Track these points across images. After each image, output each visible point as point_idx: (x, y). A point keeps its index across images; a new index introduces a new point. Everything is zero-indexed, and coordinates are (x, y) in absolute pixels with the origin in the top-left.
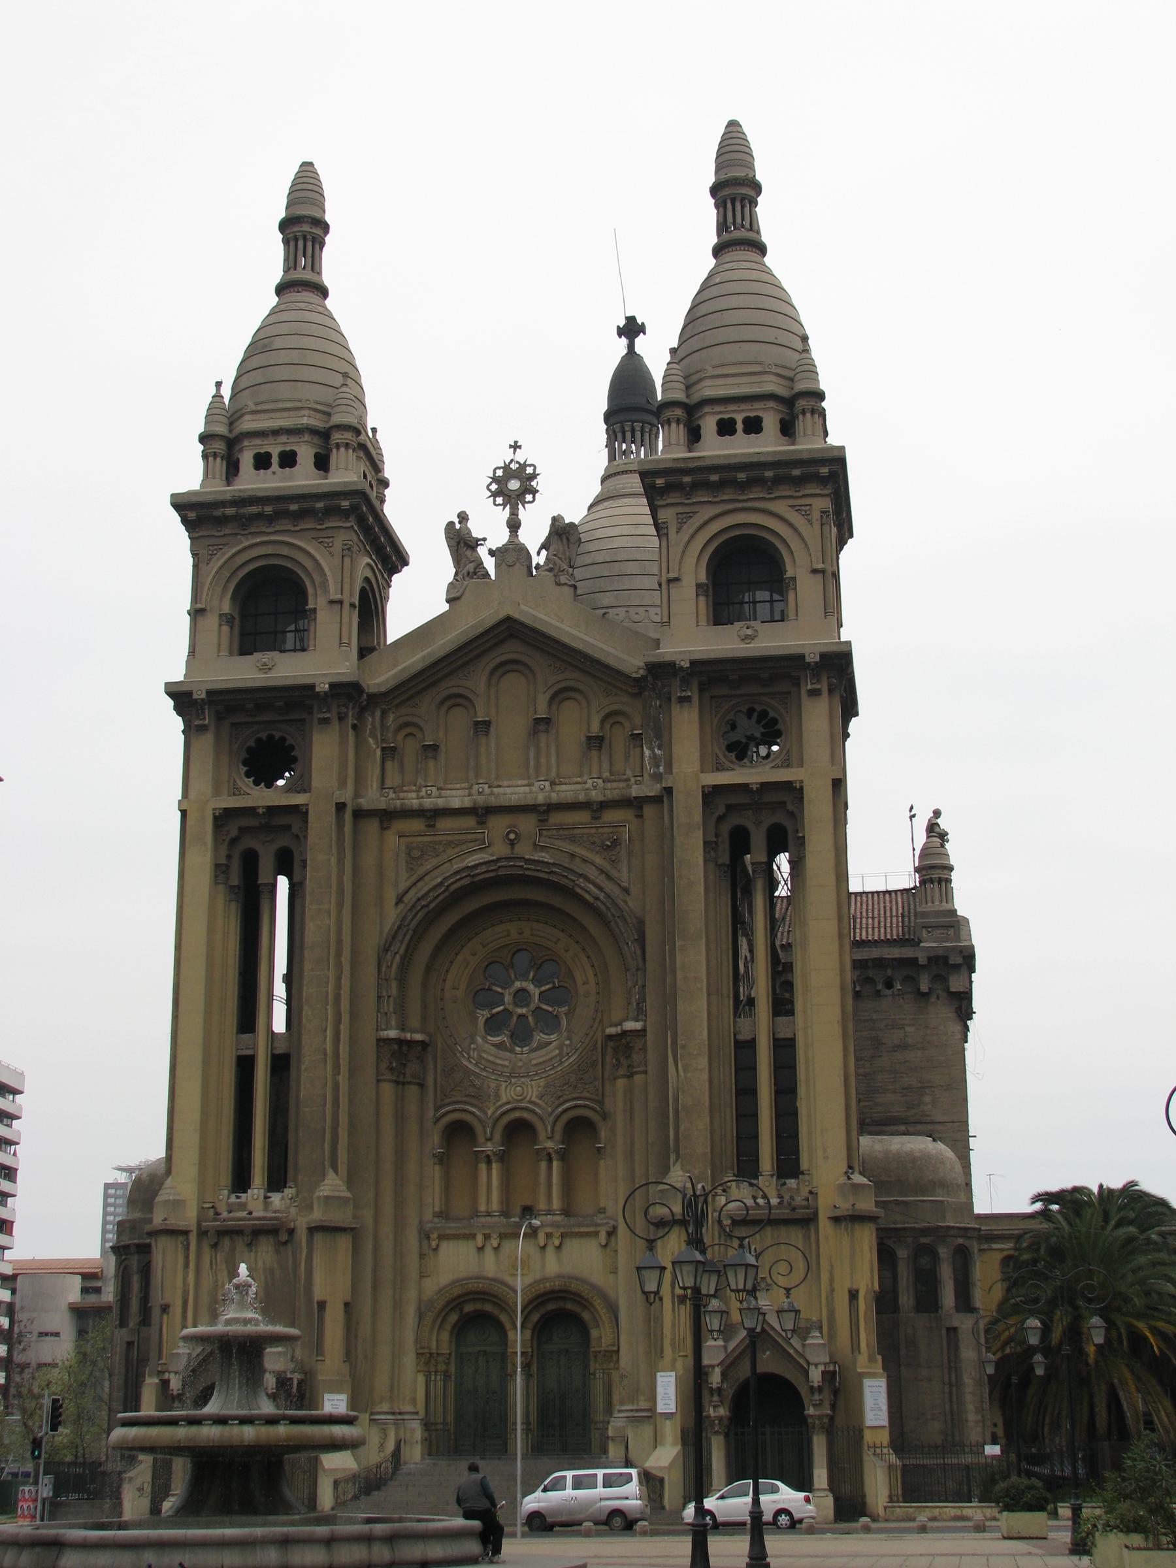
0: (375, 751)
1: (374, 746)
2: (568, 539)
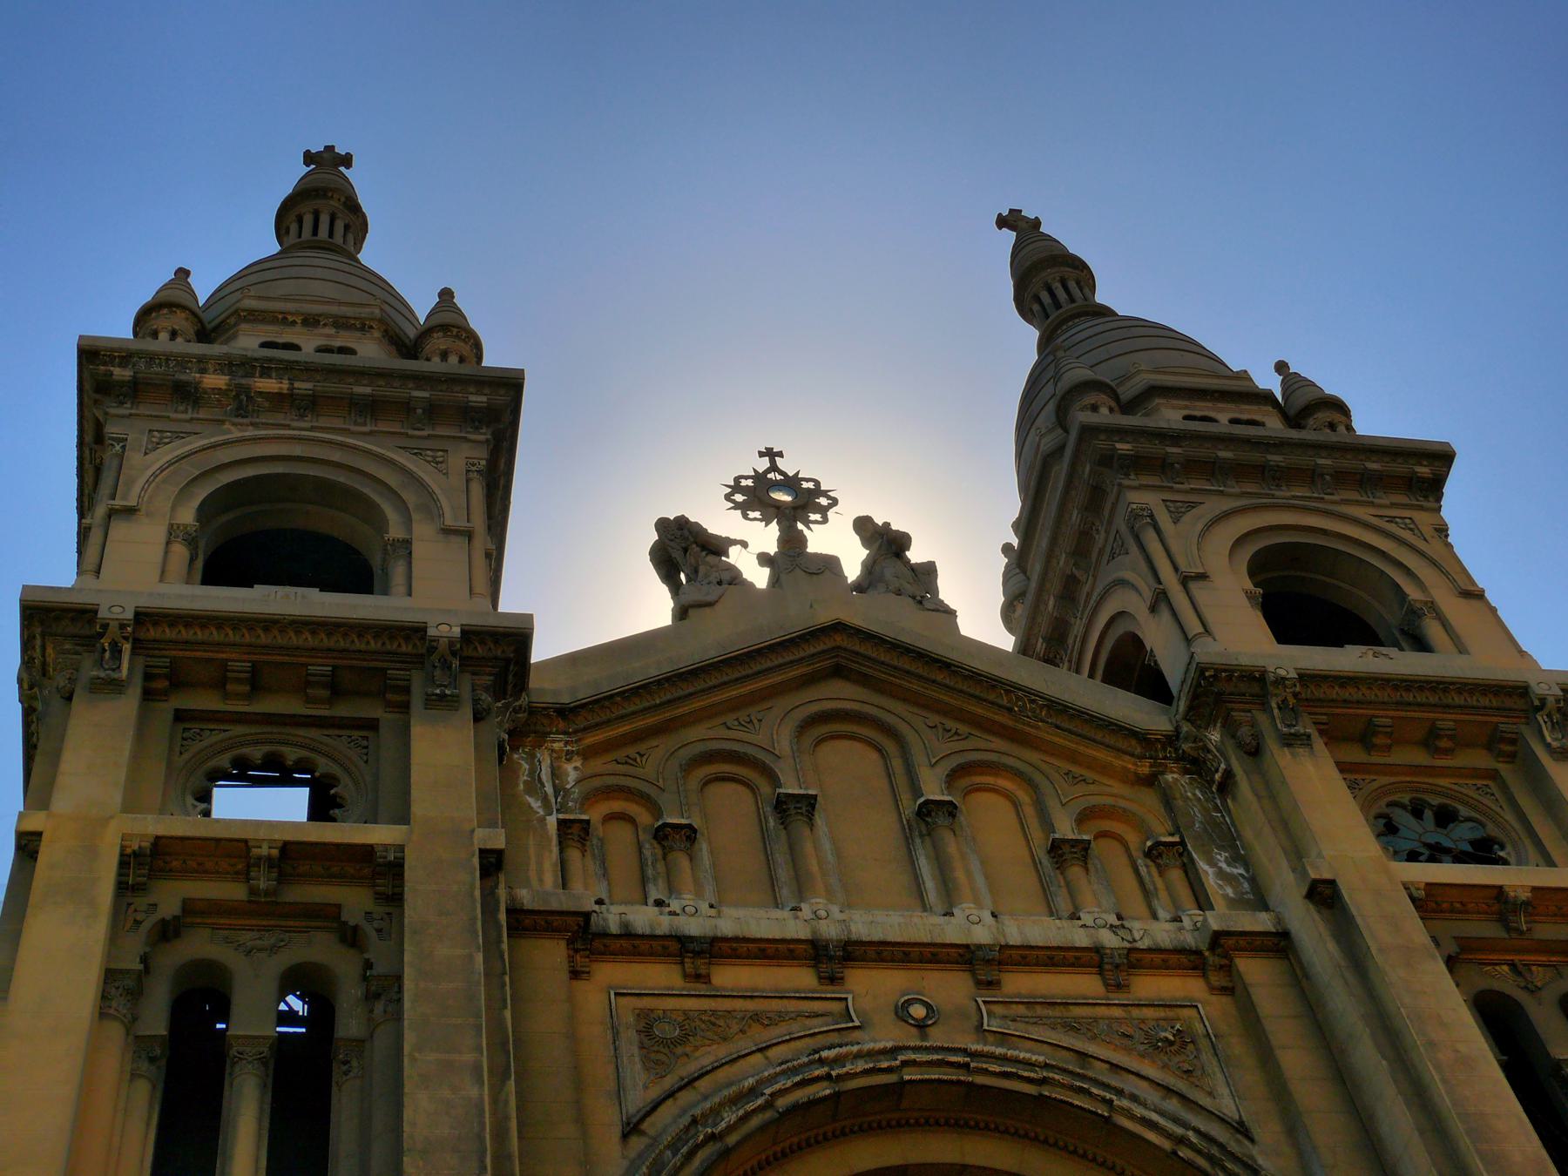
0: (542, 820)
1: (541, 812)
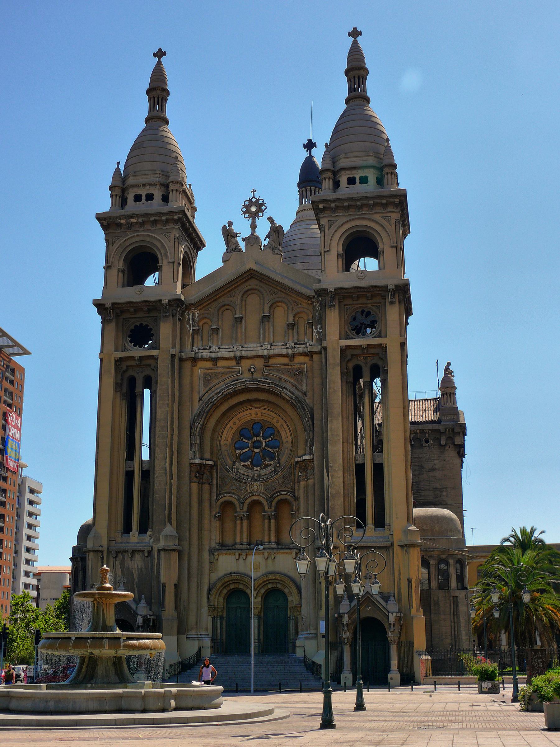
0: (189, 330)
1: (189, 328)
2: (278, 233)
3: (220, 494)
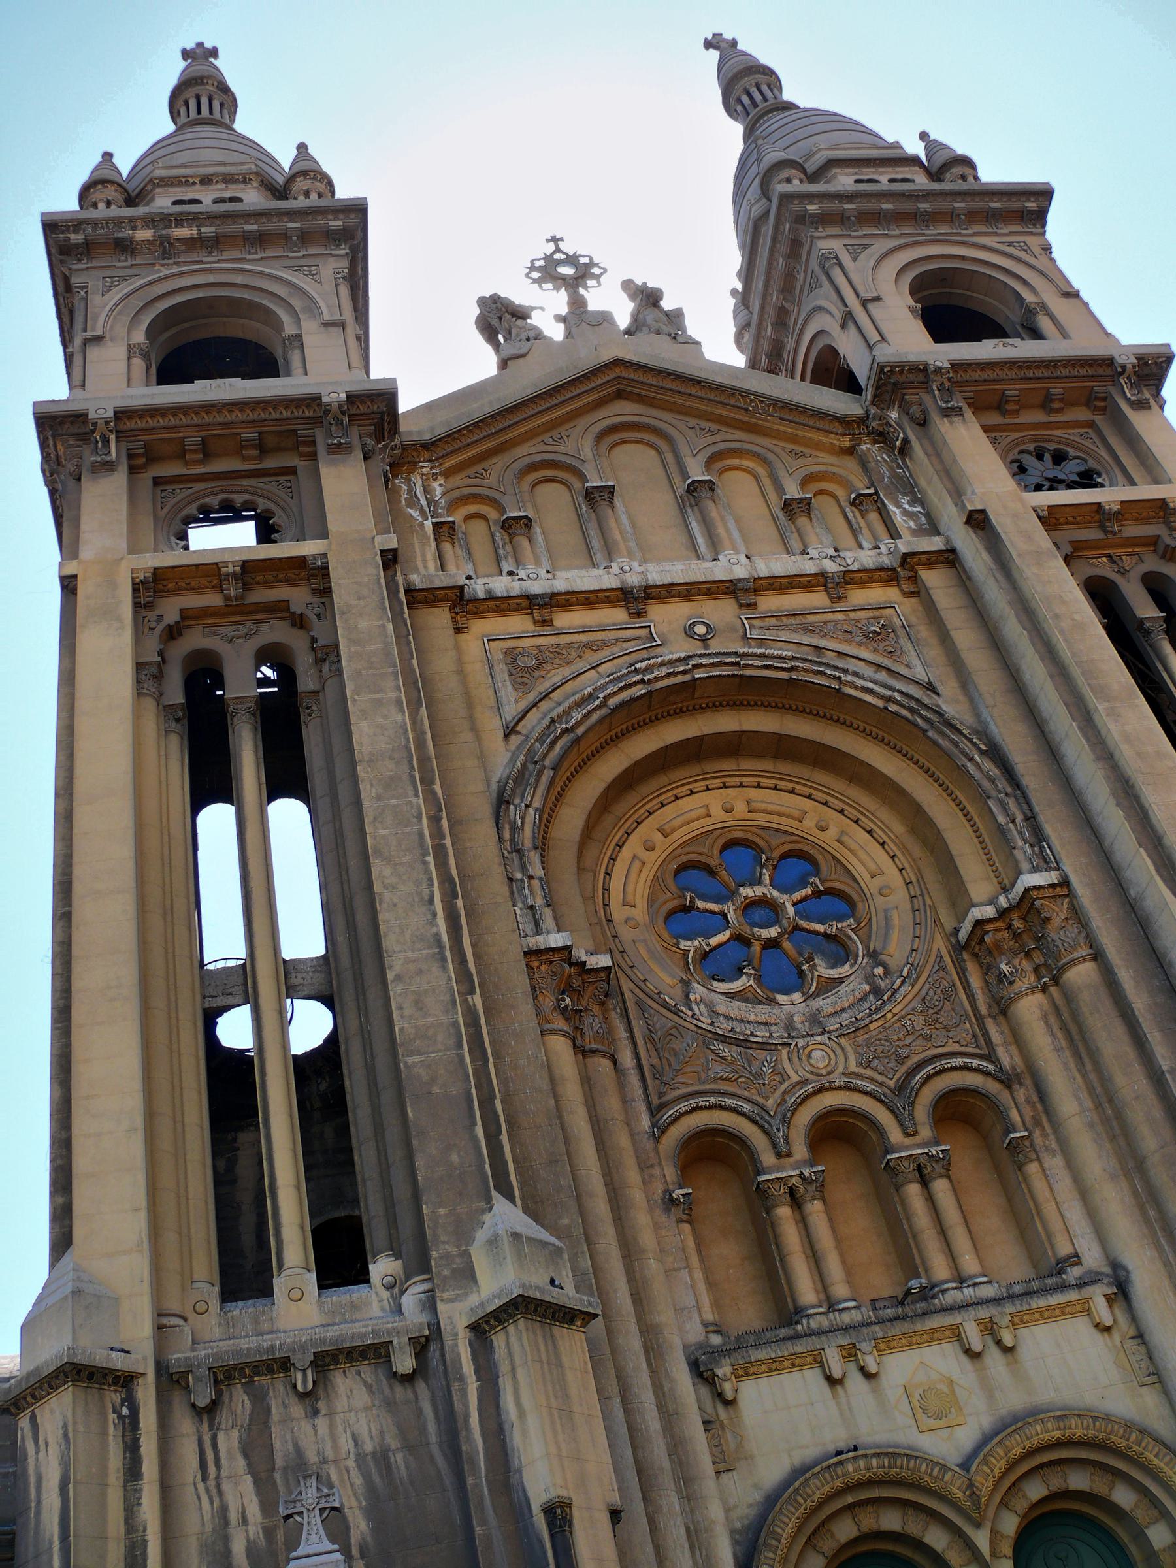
0: (422, 525)
1: (420, 519)
3: (663, 1106)
